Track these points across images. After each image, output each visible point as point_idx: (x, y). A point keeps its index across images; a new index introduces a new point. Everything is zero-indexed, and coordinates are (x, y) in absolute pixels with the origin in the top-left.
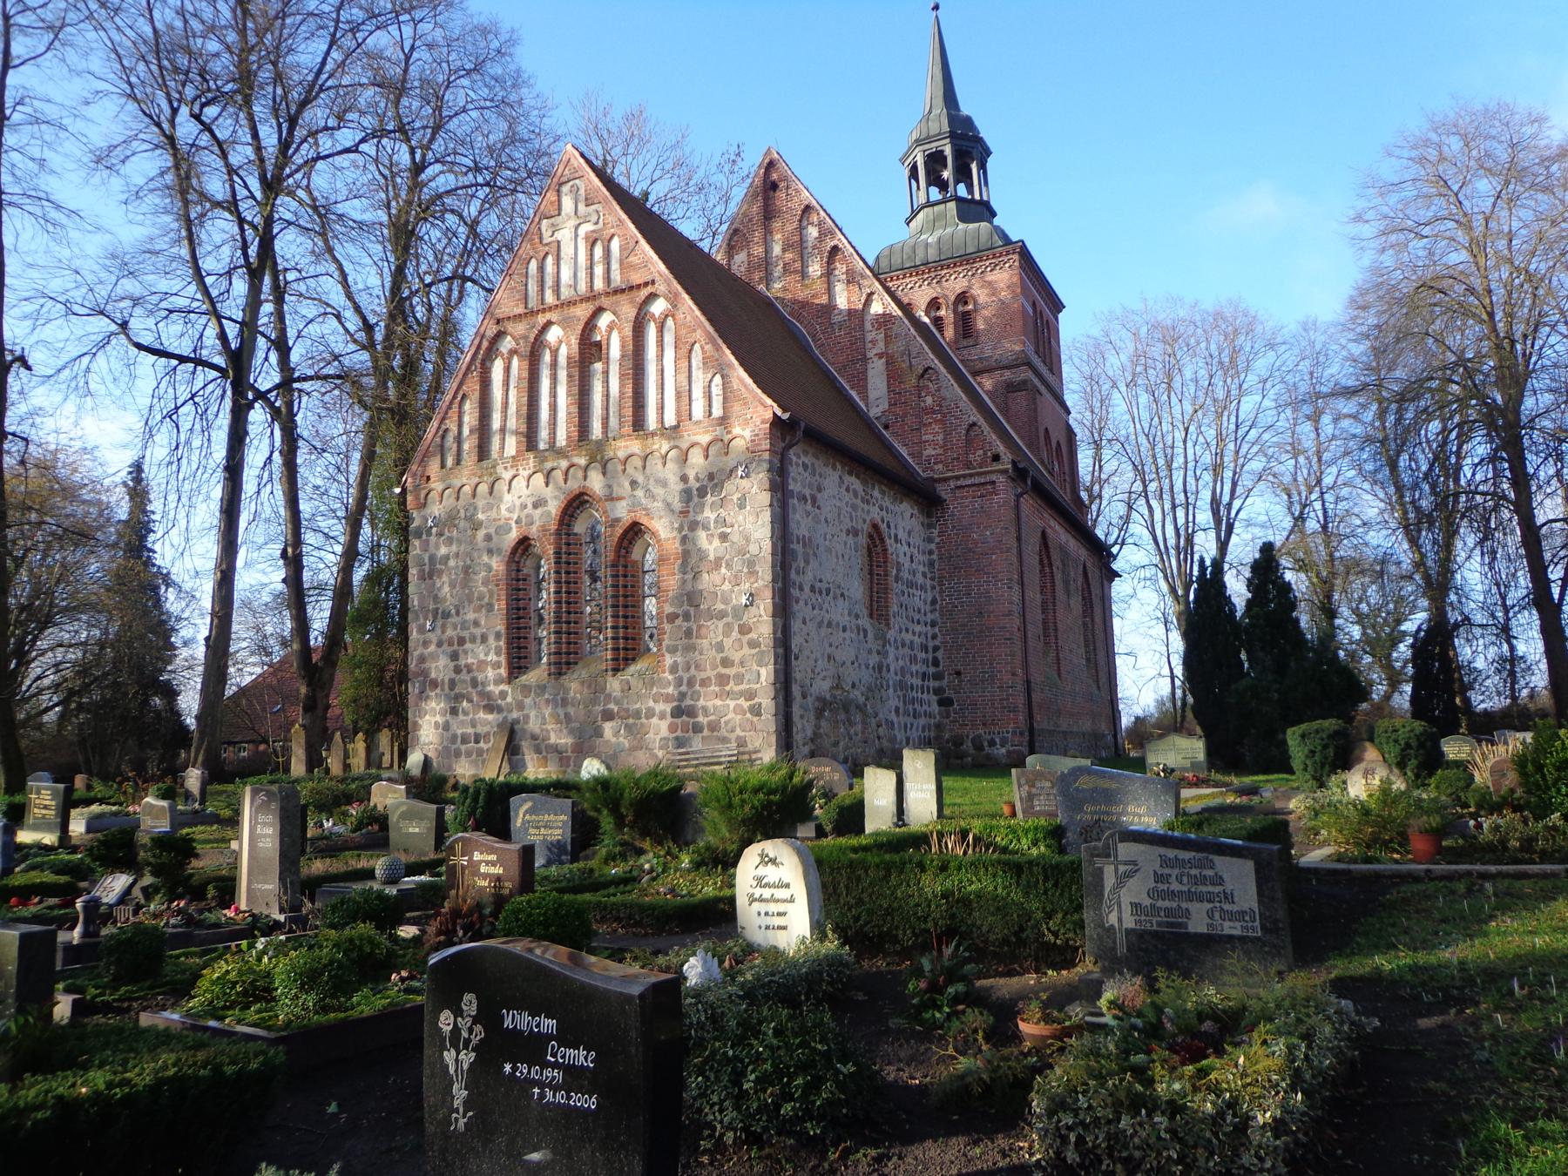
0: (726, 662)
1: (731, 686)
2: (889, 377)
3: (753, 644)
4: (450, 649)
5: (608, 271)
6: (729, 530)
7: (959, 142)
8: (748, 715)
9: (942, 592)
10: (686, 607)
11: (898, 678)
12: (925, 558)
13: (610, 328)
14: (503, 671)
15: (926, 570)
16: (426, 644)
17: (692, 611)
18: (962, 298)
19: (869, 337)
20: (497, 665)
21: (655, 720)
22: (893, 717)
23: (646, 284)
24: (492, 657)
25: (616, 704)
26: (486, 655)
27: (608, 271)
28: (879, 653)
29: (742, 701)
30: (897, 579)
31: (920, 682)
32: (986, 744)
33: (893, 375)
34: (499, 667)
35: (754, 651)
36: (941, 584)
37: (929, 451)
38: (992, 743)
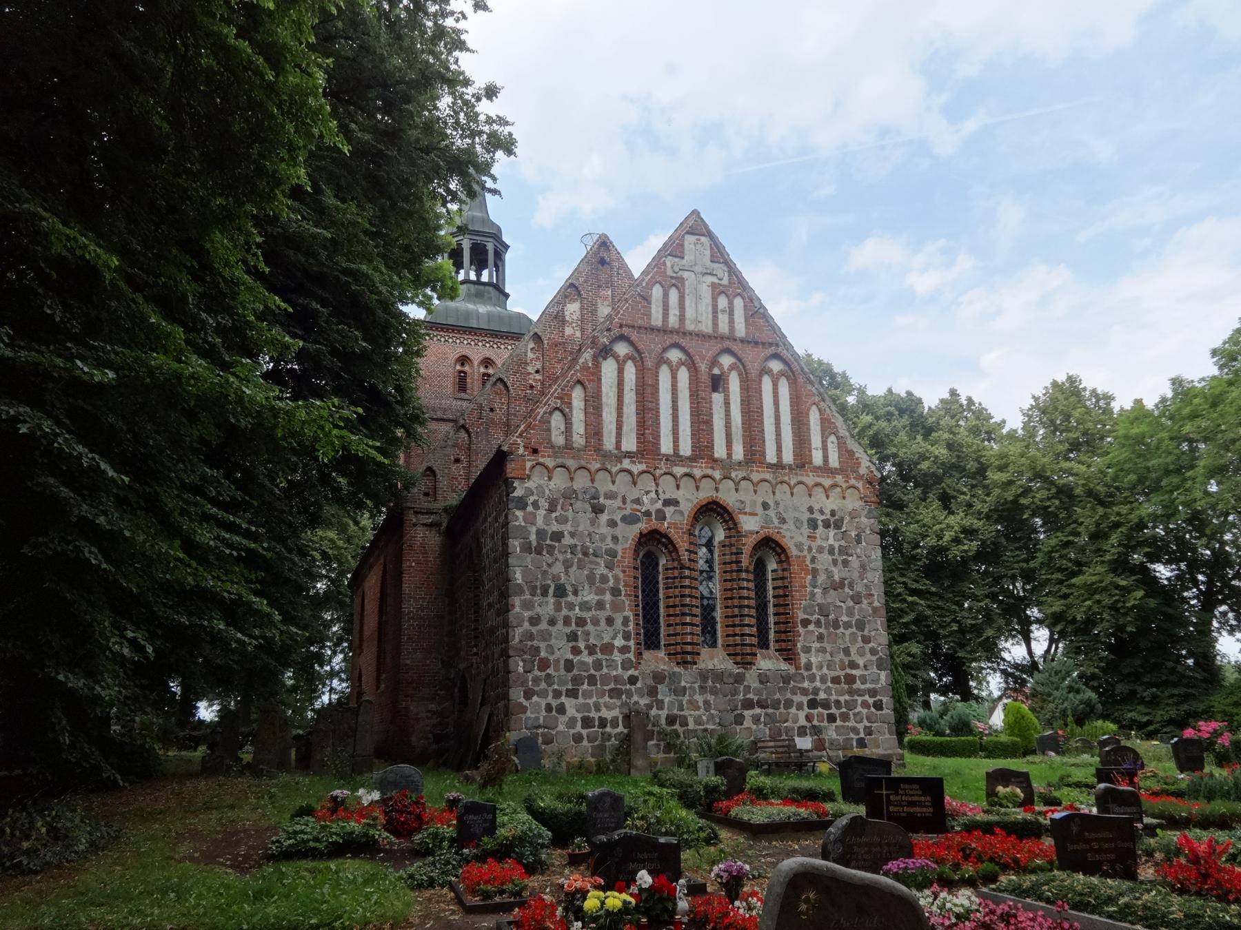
0: (853, 665)
1: (858, 685)
3: (873, 652)
4: (568, 630)
5: (731, 322)
6: (850, 558)
8: (873, 709)
10: (816, 616)
13: (732, 367)
16: (534, 621)
17: (822, 619)
20: (624, 650)
21: (793, 710)
24: (619, 642)
25: (755, 695)
26: (614, 637)
29: (867, 697)
35: (874, 658)
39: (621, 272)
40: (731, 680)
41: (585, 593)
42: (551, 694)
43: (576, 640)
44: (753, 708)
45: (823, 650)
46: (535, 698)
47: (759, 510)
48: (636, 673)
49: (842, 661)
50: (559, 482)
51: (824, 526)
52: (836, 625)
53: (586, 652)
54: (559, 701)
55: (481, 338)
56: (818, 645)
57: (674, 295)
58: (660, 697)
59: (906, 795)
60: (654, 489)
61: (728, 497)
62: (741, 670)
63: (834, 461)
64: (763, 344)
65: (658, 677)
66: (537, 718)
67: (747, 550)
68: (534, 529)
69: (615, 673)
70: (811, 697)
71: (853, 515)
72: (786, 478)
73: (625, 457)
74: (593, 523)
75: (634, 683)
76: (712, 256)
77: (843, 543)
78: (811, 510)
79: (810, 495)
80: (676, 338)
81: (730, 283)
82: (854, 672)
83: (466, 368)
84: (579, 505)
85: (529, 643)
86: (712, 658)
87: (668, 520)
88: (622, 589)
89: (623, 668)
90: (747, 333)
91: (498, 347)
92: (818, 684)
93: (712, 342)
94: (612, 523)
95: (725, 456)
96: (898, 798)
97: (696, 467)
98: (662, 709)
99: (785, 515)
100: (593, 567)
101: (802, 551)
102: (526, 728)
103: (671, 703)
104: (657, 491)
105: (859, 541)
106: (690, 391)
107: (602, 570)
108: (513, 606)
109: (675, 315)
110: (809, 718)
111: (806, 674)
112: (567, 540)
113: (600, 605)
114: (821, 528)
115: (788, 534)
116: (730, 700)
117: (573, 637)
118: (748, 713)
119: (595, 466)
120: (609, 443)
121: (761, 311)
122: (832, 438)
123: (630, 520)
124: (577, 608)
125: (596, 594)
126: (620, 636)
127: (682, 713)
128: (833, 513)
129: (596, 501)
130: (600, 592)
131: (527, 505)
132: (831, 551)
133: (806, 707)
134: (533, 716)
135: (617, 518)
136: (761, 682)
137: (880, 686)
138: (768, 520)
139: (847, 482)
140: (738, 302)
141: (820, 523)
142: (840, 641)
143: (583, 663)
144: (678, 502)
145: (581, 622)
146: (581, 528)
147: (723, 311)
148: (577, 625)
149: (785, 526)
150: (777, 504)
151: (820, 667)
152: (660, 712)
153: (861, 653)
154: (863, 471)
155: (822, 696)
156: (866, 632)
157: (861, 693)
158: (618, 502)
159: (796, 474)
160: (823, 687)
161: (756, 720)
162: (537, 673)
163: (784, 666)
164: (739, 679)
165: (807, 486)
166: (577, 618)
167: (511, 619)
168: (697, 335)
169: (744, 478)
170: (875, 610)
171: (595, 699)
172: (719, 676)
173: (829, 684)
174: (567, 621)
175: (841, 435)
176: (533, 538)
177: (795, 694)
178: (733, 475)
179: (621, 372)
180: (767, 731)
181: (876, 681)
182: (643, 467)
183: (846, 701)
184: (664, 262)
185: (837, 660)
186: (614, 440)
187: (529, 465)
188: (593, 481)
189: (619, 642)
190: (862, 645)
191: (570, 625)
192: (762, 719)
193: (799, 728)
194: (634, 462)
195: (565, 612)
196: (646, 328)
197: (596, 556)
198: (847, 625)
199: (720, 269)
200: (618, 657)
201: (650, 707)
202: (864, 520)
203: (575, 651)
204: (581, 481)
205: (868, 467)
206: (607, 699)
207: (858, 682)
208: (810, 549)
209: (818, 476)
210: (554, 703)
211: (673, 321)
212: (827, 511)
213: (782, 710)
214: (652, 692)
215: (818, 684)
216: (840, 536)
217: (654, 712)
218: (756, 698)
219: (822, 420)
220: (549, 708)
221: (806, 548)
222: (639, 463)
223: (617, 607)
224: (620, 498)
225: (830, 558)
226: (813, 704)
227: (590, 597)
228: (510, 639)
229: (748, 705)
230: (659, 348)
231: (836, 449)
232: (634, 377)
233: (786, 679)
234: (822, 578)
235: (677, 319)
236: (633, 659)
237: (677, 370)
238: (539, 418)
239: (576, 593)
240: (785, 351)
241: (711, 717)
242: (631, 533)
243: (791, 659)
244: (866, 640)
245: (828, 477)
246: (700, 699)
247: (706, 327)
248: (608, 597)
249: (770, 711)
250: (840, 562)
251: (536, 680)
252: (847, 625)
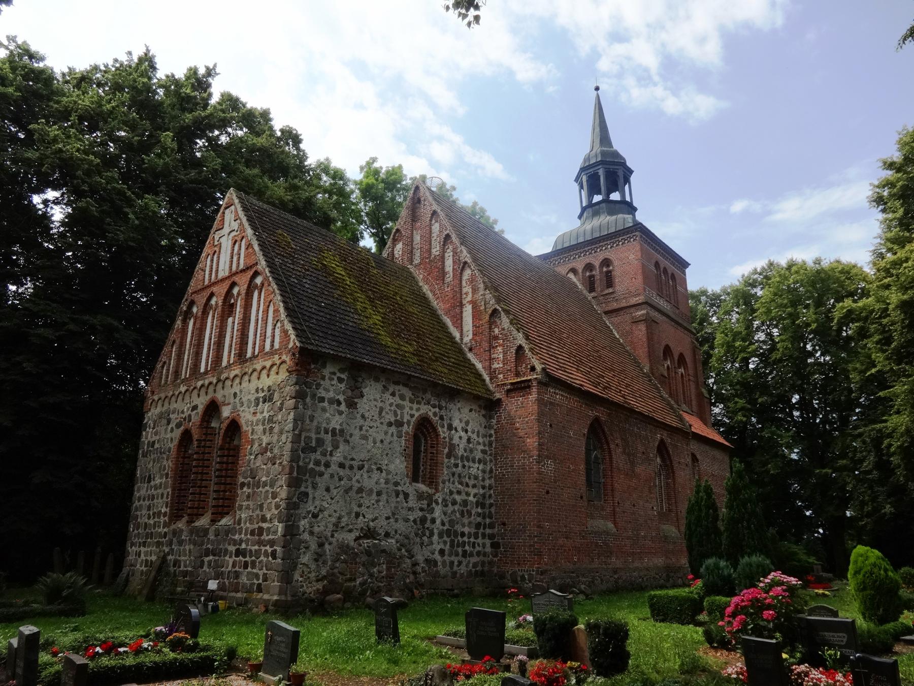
0: (264, 519)
1: (265, 537)
2: (473, 317)
7: (607, 167)
9: (496, 465)
11: (445, 528)
12: (487, 440)
15: (487, 448)
18: (606, 262)
19: (464, 290)
20: (165, 514)
22: (437, 556)
28: (421, 510)
29: (268, 548)
30: (449, 456)
31: (473, 531)
32: (519, 579)
33: (476, 315)
36: (496, 460)
37: (495, 366)
38: (523, 577)
47: (232, 400)
49: (258, 516)
50: (159, 409)
55: (582, 250)
68: (146, 442)
70: (238, 547)
83: (594, 273)
107: (165, 463)
112: (156, 446)
115: (242, 415)
137: (276, 537)
177: (229, 544)
181: (275, 532)
195: (149, 492)
201: (168, 554)
212: (265, 388)
217: (170, 557)
219: (274, 311)
226: (238, 553)
242: (178, 433)
252: (265, 484)
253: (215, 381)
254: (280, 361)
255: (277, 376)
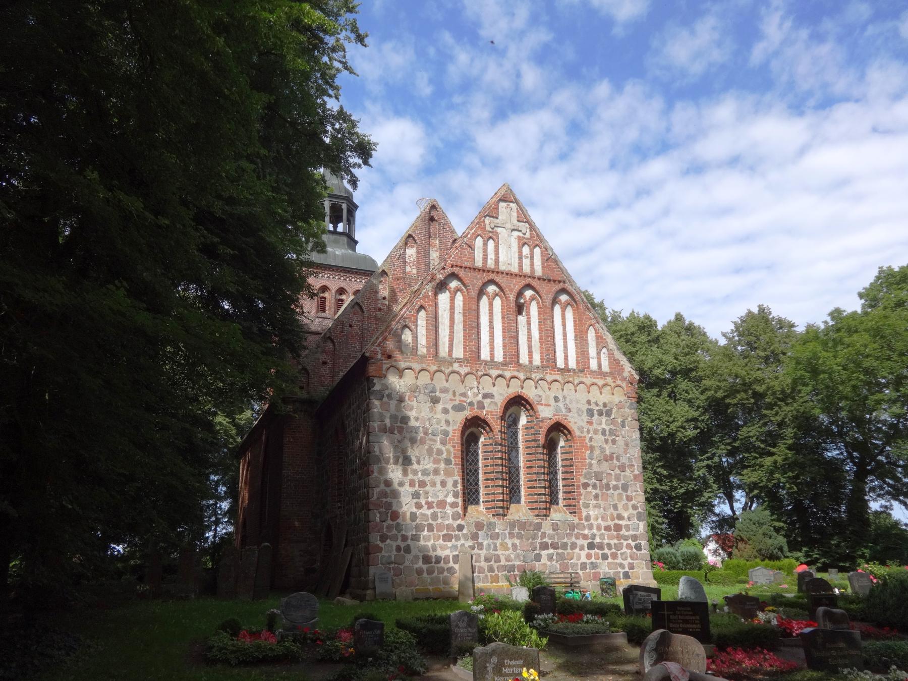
0: (620, 517)
1: (623, 532)
4: (412, 490)
5: (532, 264)
6: (617, 438)
8: (634, 550)
14: (459, 510)
20: (453, 505)
21: (577, 551)
23: (560, 282)
24: (450, 499)
26: (446, 496)
27: (532, 264)
29: (630, 541)
34: (457, 507)
35: (635, 512)
39: (446, 227)
40: (532, 528)
41: (426, 462)
42: (400, 538)
43: (419, 498)
44: (548, 549)
45: (597, 506)
46: (388, 541)
47: (552, 402)
48: (463, 523)
49: (612, 514)
51: (598, 415)
52: (608, 487)
53: (426, 507)
54: (405, 544)
56: (595, 502)
57: (491, 244)
58: (480, 540)
59: (681, 615)
60: (475, 386)
61: (530, 392)
62: (539, 521)
63: (605, 367)
64: (554, 281)
65: (479, 526)
66: (390, 556)
67: (543, 431)
69: (447, 522)
70: (590, 541)
71: (620, 406)
72: (571, 379)
73: (455, 362)
74: (432, 409)
75: (461, 530)
76: (518, 217)
77: (612, 426)
78: (589, 402)
79: (589, 392)
80: (492, 276)
81: (531, 237)
82: (621, 522)
84: (422, 397)
85: (385, 500)
86: (518, 511)
87: (486, 409)
88: (453, 459)
89: (454, 519)
90: (543, 273)
91: (350, 280)
92: (595, 531)
93: (518, 279)
94: (446, 411)
95: (527, 363)
96: (676, 617)
97: (506, 370)
98: (481, 549)
99: (570, 406)
100: (431, 443)
101: (582, 433)
102: (382, 564)
103: (489, 545)
104: (478, 387)
105: (623, 426)
106: (502, 314)
107: (438, 445)
108: (373, 472)
109: (492, 259)
110: (589, 556)
111: (586, 523)
113: (436, 472)
114: (596, 416)
115: (572, 420)
116: (532, 543)
117: (416, 495)
118: (544, 553)
119: (434, 368)
120: (443, 351)
121: (553, 257)
122: (604, 350)
123: (459, 408)
124: (420, 473)
125: (434, 463)
126: (451, 495)
127: (496, 553)
128: (605, 405)
129: (433, 394)
130: (436, 461)
131: (383, 396)
132: (604, 432)
133: (586, 549)
134: (386, 555)
135: (449, 406)
136: (554, 530)
137: (639, 532)
138: (558, 410)
139: (614, 382)
140: (537, 251)
141: (595, 412)
142: (610, 499)
143: (424, 515)
144: (493, 396)
145: (422, 484)
146: (423, 414)
147: (526, 257)
148: (419, 486)
149: (570, 414)
150: (565, 397)
151: (597, 519)
152: (480, 552)
153: (626, 508)
154: (626, 374)
155: (598, 540)
156: (629, 493)
157: (626, 538)
158: (450, 396)
159: (578, 376)
160: (599, 533)
161: (550, 558)
162: (389, 522)
163: (570, 517)
164: (538, 527)
165: (586, 385)
166: (419, 481)
167: (371, 481)
168: (507, 274)
169: (541, 379)
170: (635, 477)
171: (432, 542)
172: (523, 525)
173: (603, 531)
174: (412, 484)
175: (610, 348)
176: (387, 421)
177: (579, 538)
178: (533, 376)
179: (452, 299)
180: (558, 566)
181: (637, 529)
182: (467, 370)
183: (615, 544)
184: (484, 221)
185: (608, 513)
186: (447, 350)
187: (385, 367)
188: (432, 379)
189: (450, 499)
190: (626, 502)
191: (414, 486)
192: (554, 557)
193: (581, 564)
194: (461, 366)
195: (410, 476)
196: (470, 268)
197: (434, 435)
198: (616, 488)
199: (524, 227)
200: (449, 511)
202: (627, 410)
203: (419, 506)
204: (424, 378)
205: (630, 372)
206: (441, 542)
207: (624, 530)
208: (588, 432)
209: (594, 378)
210: (403, 545)
211: (491, 264)
212: (601, 403)
213: (569, 550)
214: (475, 537)
215: (595, 531)
216: (610, 422)
218: (550, 542)
220: (398, 548)
221: (585, 430)
222: (465, 366)
223: (448, 473)
224: (451, 392)
225: (603, 438)
226: (591, 546)
227: (430, 466)
228: (370, 497)
229: (545, 546)
230: (480, 283)
231: (607, 358)
232: (461, 303)
233: (572, 527)
234: (597, 452)
235: (493, 262)
236: (460, 512)
237: (494, 299)
238: (392, 332)
239: (418, 462)
240: (570, 287)
241: (518, 556)
242: (459, 419)
243: (575, 512)
244: (629, 499)
245: (602, 378)
246: (509, 542)
247: (515, 269)
248: (442, 466)
249: (560, 551)
250: (610, 441)
251: (389, 528)
253: (522, 376)
254: (615, 384)
255: (612, 396)
